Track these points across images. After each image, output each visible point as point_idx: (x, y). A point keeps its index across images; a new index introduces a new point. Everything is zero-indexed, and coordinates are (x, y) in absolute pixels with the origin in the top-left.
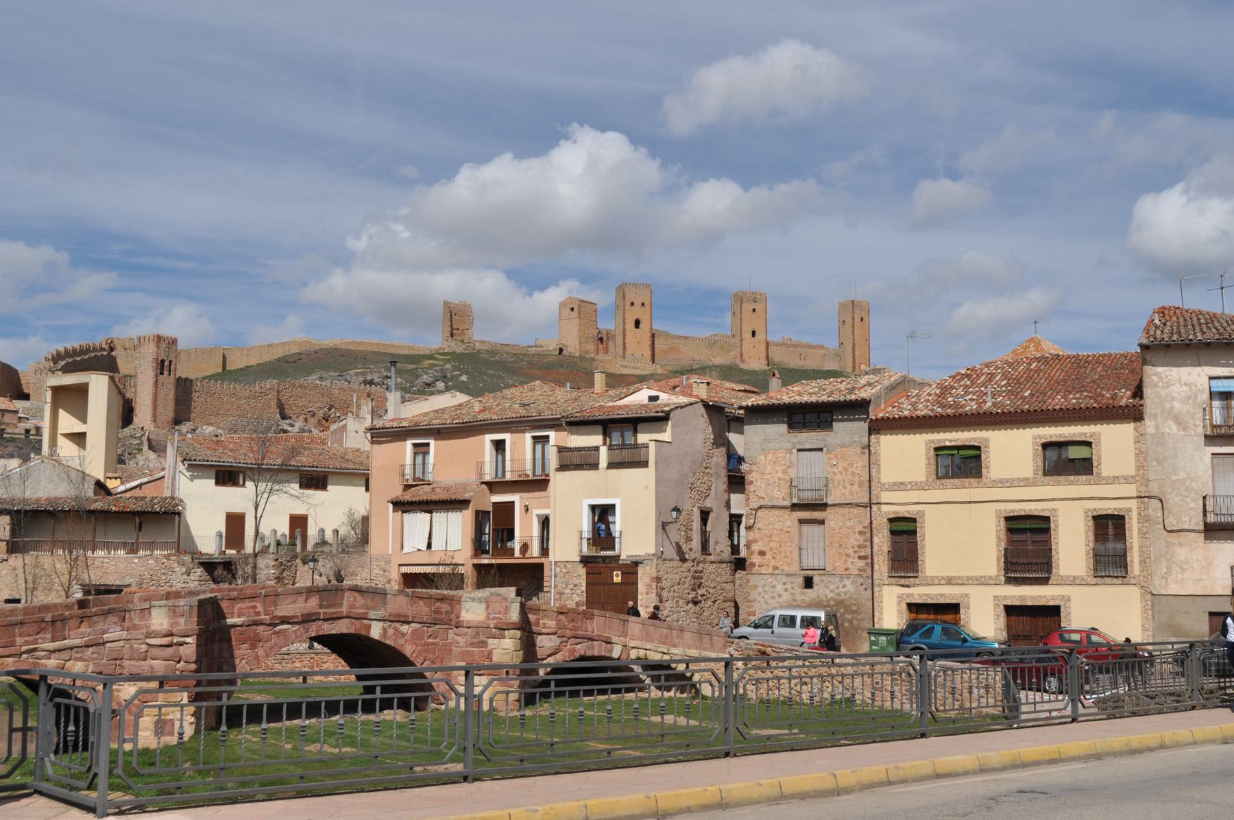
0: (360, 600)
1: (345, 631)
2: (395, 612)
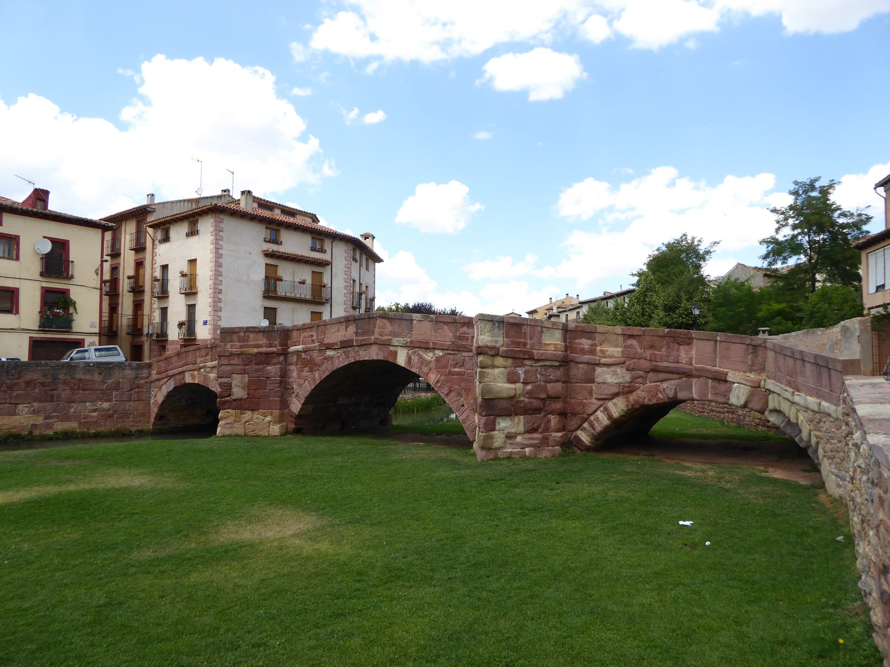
0: (389, 327)
1: (375, 358)
2: (421, 338)
